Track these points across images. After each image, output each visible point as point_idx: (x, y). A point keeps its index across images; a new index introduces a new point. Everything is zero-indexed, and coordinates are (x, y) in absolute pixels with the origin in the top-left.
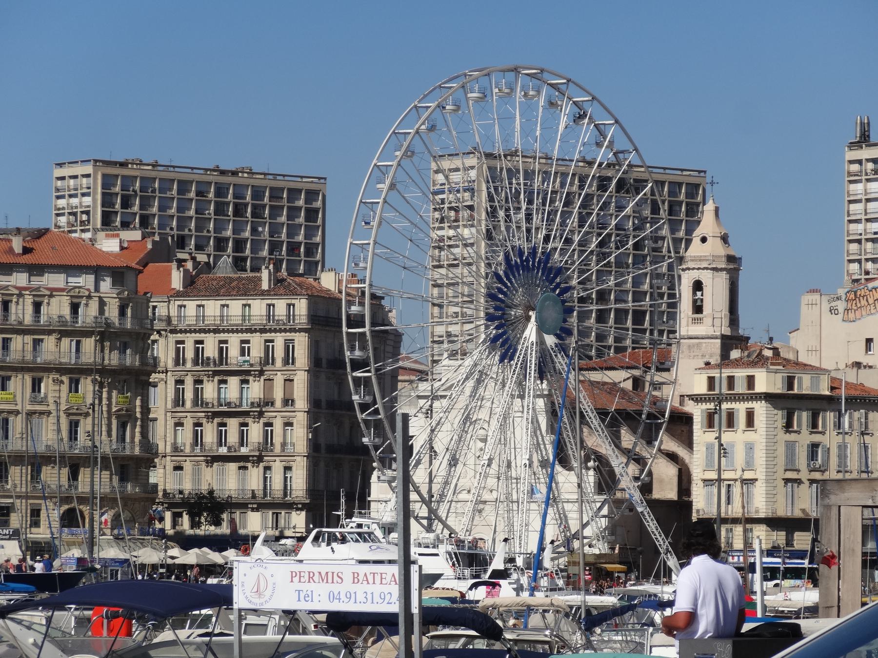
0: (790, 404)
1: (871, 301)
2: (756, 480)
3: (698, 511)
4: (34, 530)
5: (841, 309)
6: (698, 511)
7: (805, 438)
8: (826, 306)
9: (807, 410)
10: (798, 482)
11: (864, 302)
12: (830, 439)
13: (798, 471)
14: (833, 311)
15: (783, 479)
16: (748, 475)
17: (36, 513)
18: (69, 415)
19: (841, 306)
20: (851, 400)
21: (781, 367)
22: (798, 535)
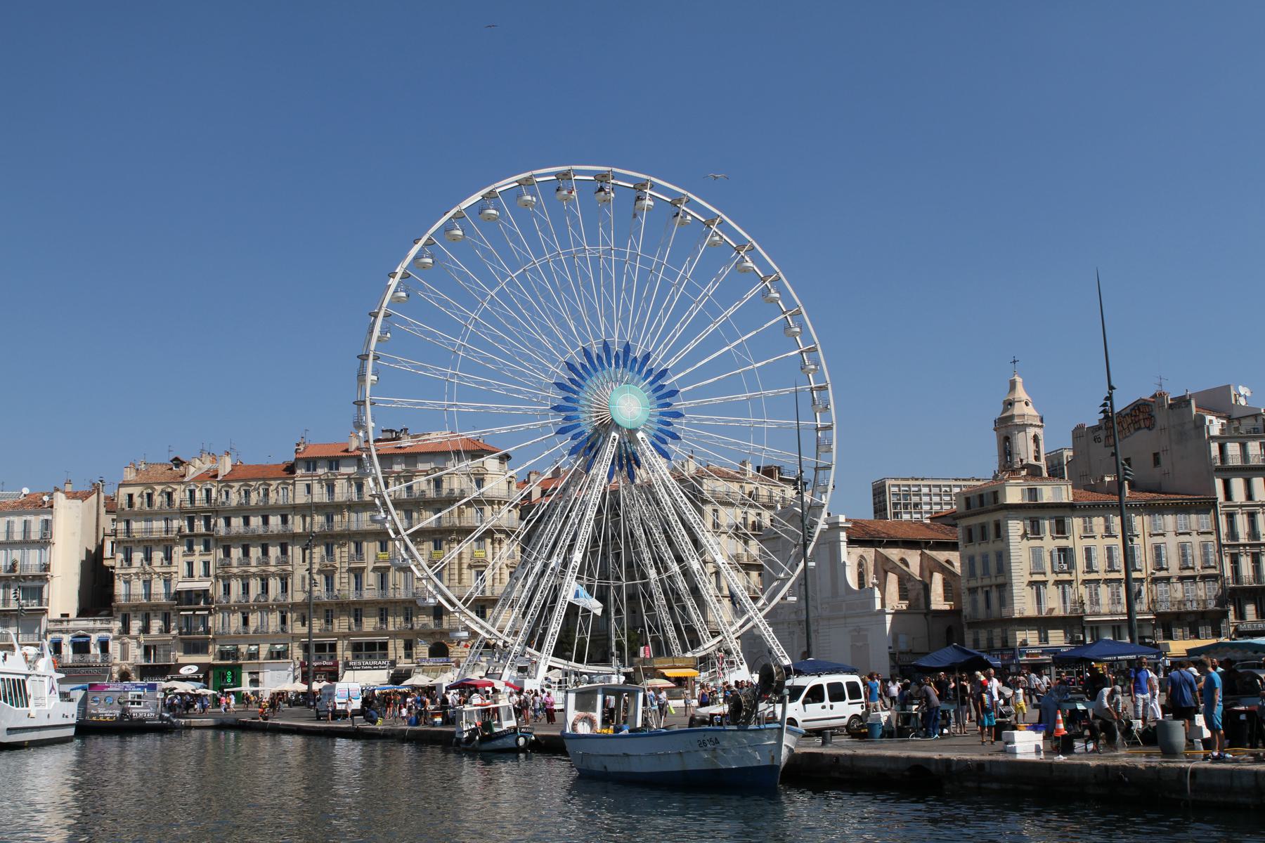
0: (1033, 514)
1: (1125, 426)
3: (966, 616)
5: (1103, 438)
6: (966, 616)
7: (1049, 543)
9: (1051, 518)
10: (1044, 583)
12: (1075, 541)
13: (1044, 574)
20: (1094, 506)
21: (1022, 481)
22: (1051, 633)
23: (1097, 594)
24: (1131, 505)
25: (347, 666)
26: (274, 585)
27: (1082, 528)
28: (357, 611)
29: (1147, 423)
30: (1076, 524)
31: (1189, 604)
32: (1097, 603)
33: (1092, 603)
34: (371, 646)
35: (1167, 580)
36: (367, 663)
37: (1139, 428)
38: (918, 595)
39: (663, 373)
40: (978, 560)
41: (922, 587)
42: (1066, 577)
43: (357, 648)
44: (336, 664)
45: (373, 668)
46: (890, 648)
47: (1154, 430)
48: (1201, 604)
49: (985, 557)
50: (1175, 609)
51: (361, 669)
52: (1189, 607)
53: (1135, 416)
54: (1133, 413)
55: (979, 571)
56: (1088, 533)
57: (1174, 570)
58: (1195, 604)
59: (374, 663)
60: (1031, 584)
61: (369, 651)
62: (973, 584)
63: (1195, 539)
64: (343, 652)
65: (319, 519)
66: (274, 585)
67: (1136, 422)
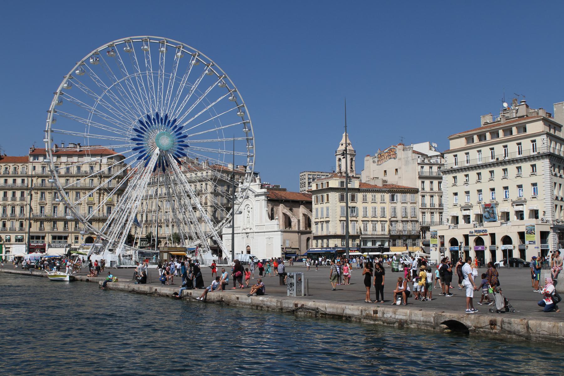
1: (385, 157)
2: (329, 221)
4: (76, 244)
5: (376, 162)
8: (371, 161)
11: (383, 158)
14: (374, 162)
15: (340, 220)
16: (327, 219)
17: (77, 238)
18: (88, 204)
19: (376, 160)
23: (366, 227)
24: (383, 190)
25: (50, 246)
26: (18, 209)
27: (362, 199)
28: (55, 221)
29: (394, 156)
30: (360, 196)
31: (404, 232)
32: (367, 230)
33: (364, 230)
34: (60, 238)
35: (397, 221)
36: (58, 245)
37: (391, 158)
38: (295, 224)
39: (181, 128)
40: (319, 210)
41: (297, 220)
42: (354, 219)
43: (54, 238)
44: (45, 245)
45: (61, 247)
46: (282, 245)
47: (396, 159)
48: (409, 232)
49: (322, 209)
50: (398, 234)
51: (55, 248)
52: (404, 233)
53: (390, 153)
54: (389, 152)
55: (319, 216)
56: (365, 200)
57: (399, 218)
58: (406, 232)
59: (62, 245)
60: (341, 221)
61: (59, 238)
62: (317, 220)
63: (409, 206)
64: (48, 239)
65: (40, 180)
66: (18, 209)
67: (390, 156)
